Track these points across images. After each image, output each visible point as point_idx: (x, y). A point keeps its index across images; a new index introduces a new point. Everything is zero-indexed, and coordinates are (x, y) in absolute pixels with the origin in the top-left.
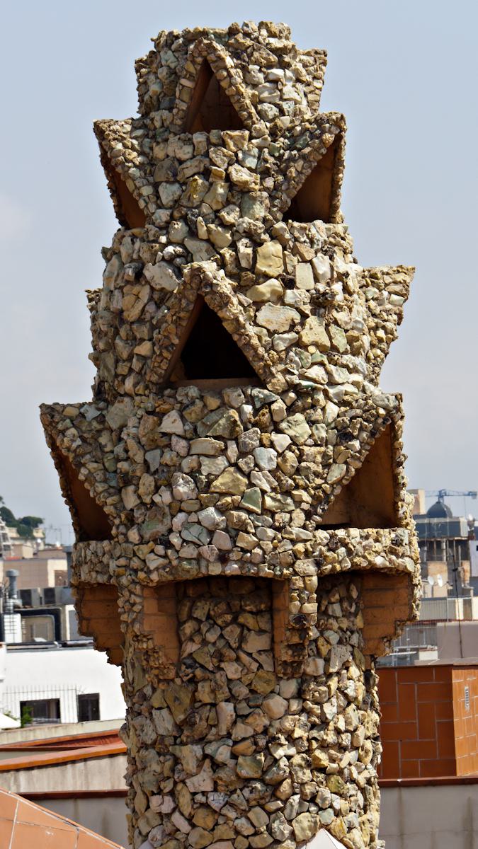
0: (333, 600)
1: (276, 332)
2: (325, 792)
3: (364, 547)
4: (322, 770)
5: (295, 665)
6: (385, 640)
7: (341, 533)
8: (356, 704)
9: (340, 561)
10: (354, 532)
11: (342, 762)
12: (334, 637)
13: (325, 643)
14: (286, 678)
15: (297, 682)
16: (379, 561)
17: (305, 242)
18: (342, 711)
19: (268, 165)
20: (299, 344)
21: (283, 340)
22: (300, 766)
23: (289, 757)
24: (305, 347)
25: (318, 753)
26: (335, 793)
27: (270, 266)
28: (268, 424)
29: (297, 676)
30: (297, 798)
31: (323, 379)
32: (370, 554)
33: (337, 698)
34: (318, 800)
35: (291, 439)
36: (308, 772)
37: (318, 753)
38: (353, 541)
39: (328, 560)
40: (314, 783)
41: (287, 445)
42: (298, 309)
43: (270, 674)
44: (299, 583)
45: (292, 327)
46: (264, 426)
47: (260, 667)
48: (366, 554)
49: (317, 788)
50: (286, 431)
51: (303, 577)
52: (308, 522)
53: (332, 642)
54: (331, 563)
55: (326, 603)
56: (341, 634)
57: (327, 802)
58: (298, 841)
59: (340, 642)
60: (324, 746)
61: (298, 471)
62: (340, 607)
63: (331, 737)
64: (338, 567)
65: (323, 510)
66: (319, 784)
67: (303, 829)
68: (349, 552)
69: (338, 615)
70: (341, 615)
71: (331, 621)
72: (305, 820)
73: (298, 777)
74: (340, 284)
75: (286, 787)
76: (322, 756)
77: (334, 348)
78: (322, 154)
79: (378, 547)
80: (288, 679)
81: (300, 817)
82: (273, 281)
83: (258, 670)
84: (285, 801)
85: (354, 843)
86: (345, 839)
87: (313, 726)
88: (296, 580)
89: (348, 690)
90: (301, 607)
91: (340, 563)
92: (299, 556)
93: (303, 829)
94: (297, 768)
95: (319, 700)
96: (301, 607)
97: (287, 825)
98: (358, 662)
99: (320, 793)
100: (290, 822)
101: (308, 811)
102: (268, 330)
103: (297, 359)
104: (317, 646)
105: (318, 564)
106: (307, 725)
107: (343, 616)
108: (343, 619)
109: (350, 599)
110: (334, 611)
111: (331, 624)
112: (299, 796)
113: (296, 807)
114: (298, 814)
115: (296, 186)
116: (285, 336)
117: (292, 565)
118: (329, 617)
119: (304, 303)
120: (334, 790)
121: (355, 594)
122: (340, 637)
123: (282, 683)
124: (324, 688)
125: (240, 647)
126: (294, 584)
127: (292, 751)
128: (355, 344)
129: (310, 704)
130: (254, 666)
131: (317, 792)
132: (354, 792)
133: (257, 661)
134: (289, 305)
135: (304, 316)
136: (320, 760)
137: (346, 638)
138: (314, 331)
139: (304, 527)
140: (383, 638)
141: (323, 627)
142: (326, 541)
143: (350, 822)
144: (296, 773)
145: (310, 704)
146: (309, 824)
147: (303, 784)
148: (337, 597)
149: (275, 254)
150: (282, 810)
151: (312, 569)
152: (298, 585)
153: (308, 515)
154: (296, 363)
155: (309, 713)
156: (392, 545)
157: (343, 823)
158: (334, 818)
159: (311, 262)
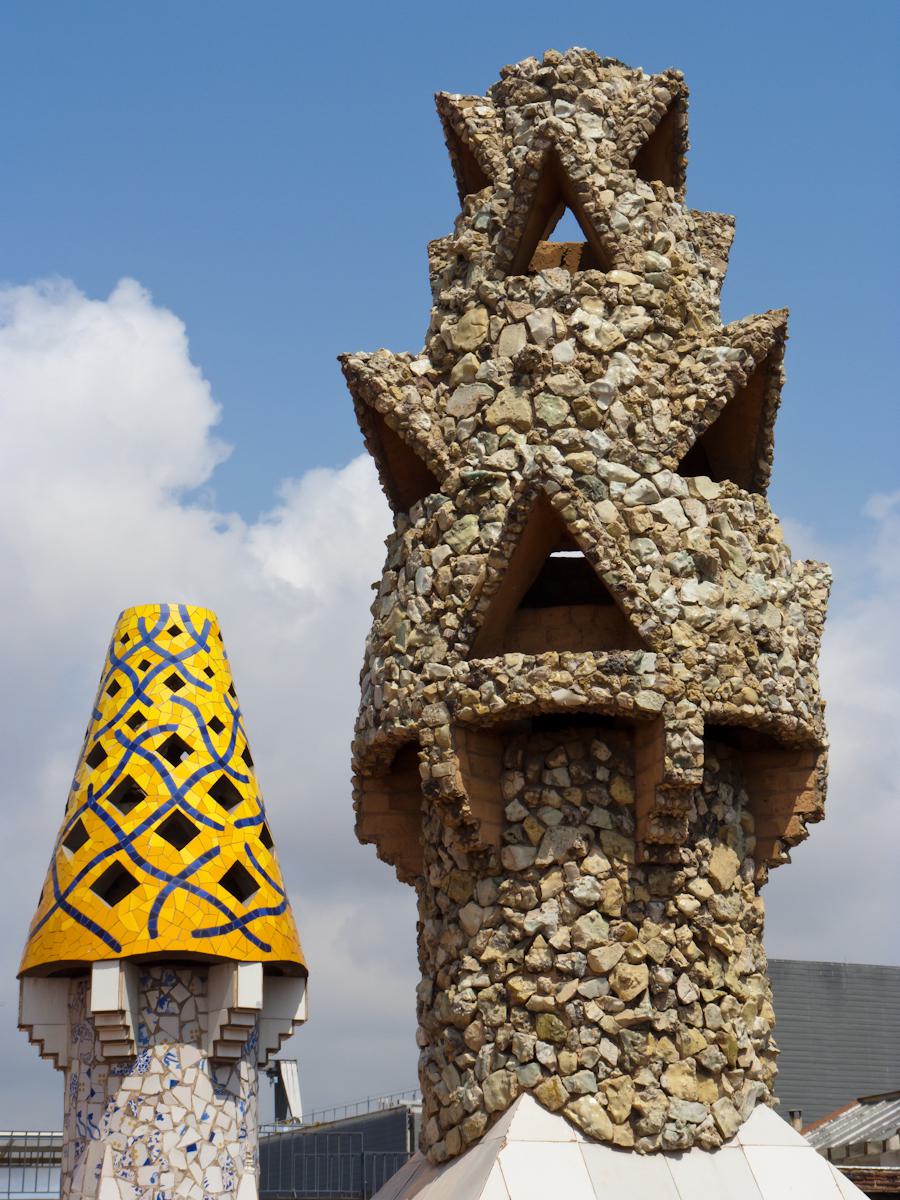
0: (552, 763)
1: (462, 417)
2: (528, 1040)
3: (531, 679)
4: (521, 1005)
5: (481, 856)
6: (651, 816)
7: (488, 663)
8: (601, 910)
9: (489, 702)
10: (516, 659)
11: (560, 995)
12: (552, 817)
13: (536, 825)
14: (479, 877)
15: (494, 882)
16: (560, 695)
17: (523, 297)
18: (565, 920)
19: (497, 218)
20: (483, 427)
21: (466, 425)
22: (489, 1000)
23: (477, 989)
24: (492, 428)
25: (517, 983)
26: (549, 1041)
27: (468, 338)
28: (434, 536)
29: (490, 873)
30: (488, 1048)
31: (508, 464)
32: (541, 686)
33: (560, 902)
34: (516, 1051)
35: (452, 549)
36: (502, 1010)
37: (517, 983)
38: (509, 671)
39: (464, 701)
40: (509, 1025)
41: (445, 556)
42: (492, 384)
43: (466, 875)
44: (427, 737)
45: (481, 405)
46: (430, 540)
47: (455, 866)
48: (534, 688)
49: (512, 1032)
50: (448, 541)
51: (433, 728)
52: (448, 653)
53: (548, 823)
54: (470, 705)
55: (536, 768)
56: (568, 811)
57: (525, 1053)
58: (489, 1111)
59: (566, 822)
60: (532, 973)
61: (453, 588)
62: (566, 774)
63: (538, 957)
64: (481, 709)
65: (466, 633)
66: (516, 1026)
67: (494, 1094)
68: (500, 688)
69: (562, 784)
70: (568, 785)
71: (545, 793)
72: (497, 1080)
73: (487, 1017)
74: (573, 340)
75: (473, 1031)
76: (522, 987)
77: (539, 423)
78: (532, 181)
79: (560, 676)
80: (483, 878)
81: (493, 1077)
82: (469, 355)
83: (451, 870)
84: (475, 1054)
85: (580, 1117)
86: (566, 1110)
87: (515, 943)
88: (423, 733)
89: (576, 890)
90: (431, 769)
91: (487, 702)
92: (430, 700)
93: (494, 1094)
94: (487, 1004)
95: (522, 906)
96: (431, 769)
97: (478, 1088)
98: (608, 850)
99: (515, 1040)
100: (480, 1083)
101: (504, 1067)
102: (455, 418)
103: (481, 447)
104: (524, 833)
105: (450, 707)
106: (503, 942)
107: (572, 785)
108: (573, 789)
109: (592, 763)
110: (554, 779)
111: (546, 797)
112: (493, 1045)
113: (488, 1061)
114: (492, 1071)
115: (511, 230)
116: (471, 419)
117: (419, 715)
118: (545, 786)
119: (500, 374)
120: (543, 1036)
121: (603, 753)
122: (565, 817)
123: (479, 884)
124: (530, 888)
125: (441, 843)
126: (423, 739)
127: (484, 979)
128: (581, 413)
129: (509, 912)
130: (448, 864)
131: (512, 1038)
132: (592, 1041)
133: (451, 858)
134: (482, 380)
135: (498, 389)
136: (517, 991)
137: (574, 816)
138: (513, 404)
139: (445, 662)
140: (649, 813)
141: (535, 802)
142: (463, 675)
143: (573, 1084)
144: (486, 1012)
145: (509, 912)
146: (502, 1086)
147: (495, 1028)
148: (562, 758)
149: (475, 322)
150: (472, 1066)
151: (442, 715)
152: (426, 739)
153: (451, 643)
154: (477, 451)
155: (511, 925)
156: (599, 673)
157: (560, 1086)
158: (540, 1076)
159: (523, 320)
